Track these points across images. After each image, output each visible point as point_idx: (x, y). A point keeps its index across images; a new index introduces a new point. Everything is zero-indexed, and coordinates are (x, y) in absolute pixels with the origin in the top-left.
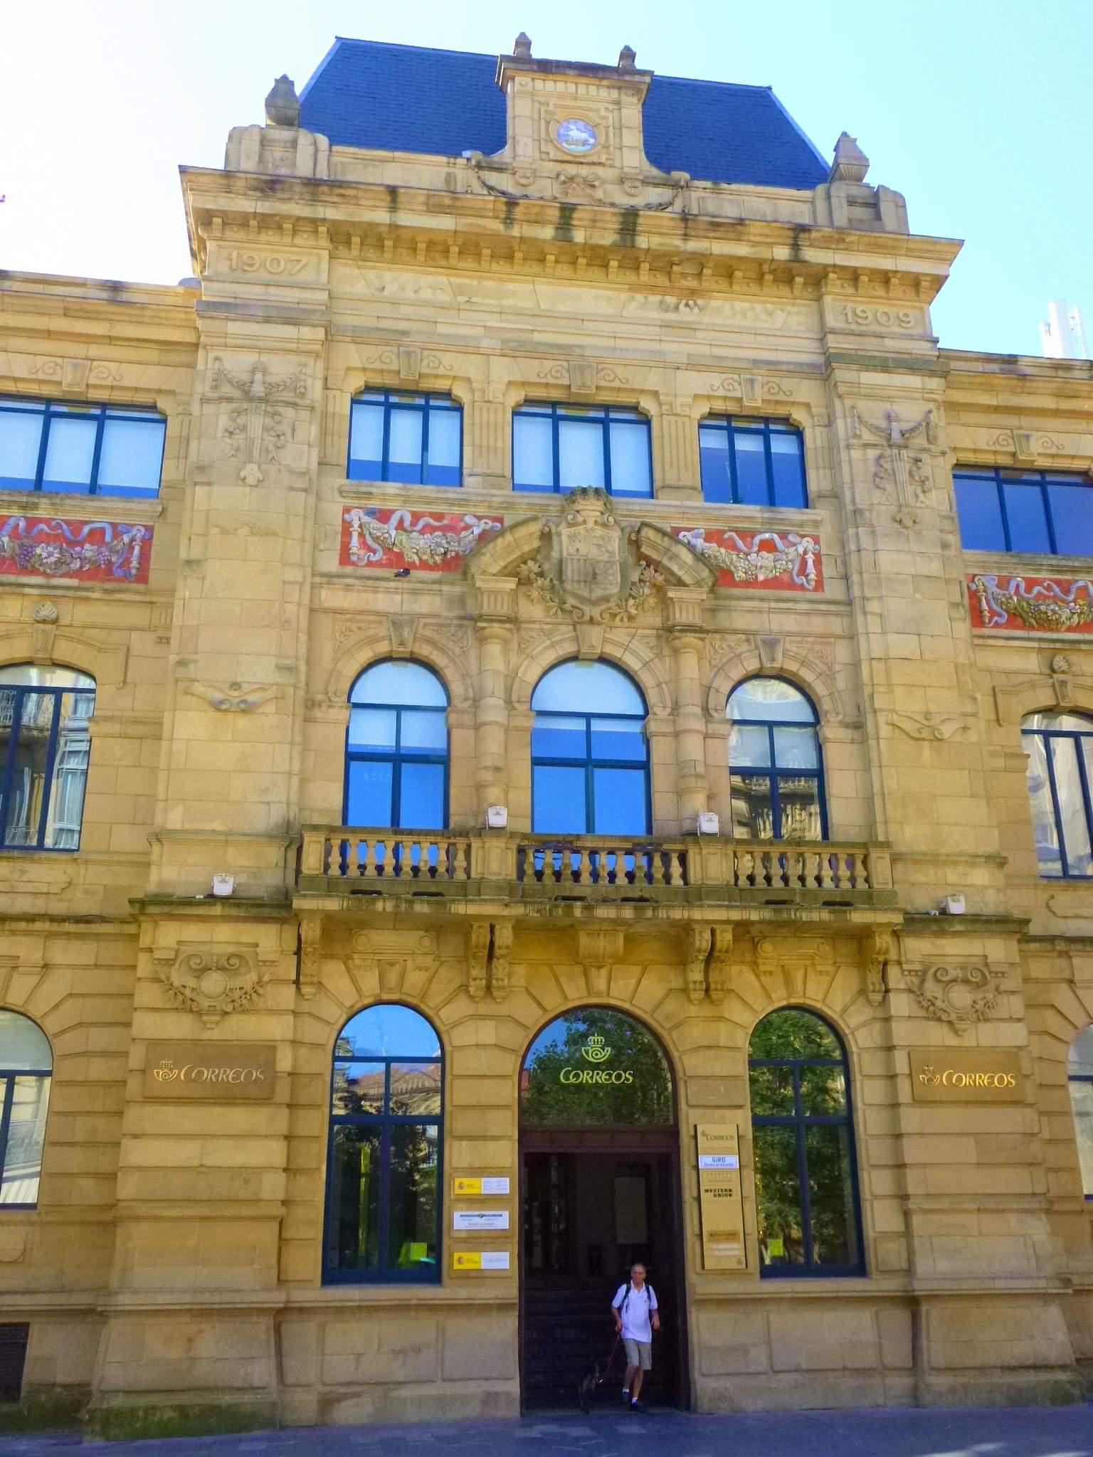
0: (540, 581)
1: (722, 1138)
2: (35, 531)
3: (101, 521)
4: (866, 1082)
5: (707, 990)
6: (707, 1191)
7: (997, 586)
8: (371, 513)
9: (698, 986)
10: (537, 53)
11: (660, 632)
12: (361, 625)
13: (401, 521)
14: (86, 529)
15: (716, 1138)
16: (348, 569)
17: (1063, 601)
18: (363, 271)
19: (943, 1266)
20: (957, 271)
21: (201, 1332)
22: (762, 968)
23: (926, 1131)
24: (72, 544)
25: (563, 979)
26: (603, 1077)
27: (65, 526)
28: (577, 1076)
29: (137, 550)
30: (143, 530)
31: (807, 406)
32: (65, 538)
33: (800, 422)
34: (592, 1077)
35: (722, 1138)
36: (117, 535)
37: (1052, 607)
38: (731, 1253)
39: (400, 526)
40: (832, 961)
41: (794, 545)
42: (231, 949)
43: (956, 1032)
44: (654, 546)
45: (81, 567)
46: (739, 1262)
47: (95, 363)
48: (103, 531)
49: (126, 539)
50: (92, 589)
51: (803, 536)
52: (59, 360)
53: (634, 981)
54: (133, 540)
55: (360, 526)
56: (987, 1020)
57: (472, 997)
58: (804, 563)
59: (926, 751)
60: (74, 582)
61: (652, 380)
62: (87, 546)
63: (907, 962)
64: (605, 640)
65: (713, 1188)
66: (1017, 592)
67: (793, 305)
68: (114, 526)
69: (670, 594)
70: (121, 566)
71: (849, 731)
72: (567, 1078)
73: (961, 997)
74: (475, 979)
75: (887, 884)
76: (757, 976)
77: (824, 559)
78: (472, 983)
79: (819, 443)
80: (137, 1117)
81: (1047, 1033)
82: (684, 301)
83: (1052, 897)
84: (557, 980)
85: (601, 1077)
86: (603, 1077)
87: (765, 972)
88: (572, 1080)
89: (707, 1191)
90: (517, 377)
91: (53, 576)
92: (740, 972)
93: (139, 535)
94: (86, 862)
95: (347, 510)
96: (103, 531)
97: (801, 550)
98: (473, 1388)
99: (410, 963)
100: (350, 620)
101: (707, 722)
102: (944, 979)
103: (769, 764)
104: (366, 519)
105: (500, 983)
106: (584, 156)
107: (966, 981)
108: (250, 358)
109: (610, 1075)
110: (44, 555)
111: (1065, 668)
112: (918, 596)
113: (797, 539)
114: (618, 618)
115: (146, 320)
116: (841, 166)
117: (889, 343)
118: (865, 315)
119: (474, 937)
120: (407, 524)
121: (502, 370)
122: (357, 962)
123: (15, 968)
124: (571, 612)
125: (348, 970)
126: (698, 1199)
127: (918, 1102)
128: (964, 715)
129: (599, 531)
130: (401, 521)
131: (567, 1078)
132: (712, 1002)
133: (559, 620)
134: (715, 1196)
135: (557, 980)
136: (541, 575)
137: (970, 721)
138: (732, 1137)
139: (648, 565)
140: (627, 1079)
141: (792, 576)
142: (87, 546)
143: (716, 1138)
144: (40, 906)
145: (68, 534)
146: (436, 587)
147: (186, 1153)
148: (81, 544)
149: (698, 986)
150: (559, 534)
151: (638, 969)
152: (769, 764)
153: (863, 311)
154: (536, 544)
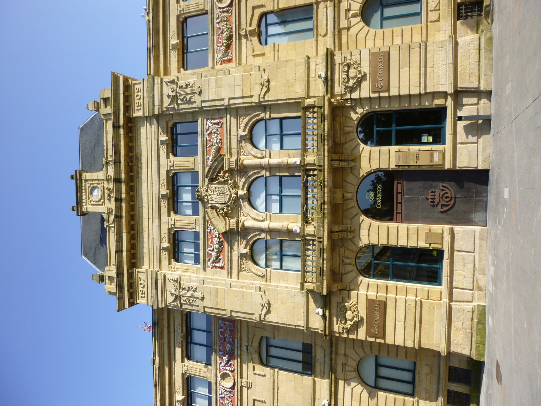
0: (225, 210)
1: (399, 157)
2: (222, 349)
3: (218, 332)
4: (381, 107)
5: (351, 161)
6: (417, 163)
7: (220, 54)
8: (209, 260)
9: (350, 164)
10: (75, 204)
11: (239, 172)
12: (242, 264)
13: (210, 250)
14: (221, 336)
15: (399, 159)
16: (226, 267)
17: (223, 30)
18: (141, 258)
19: (443, 80)
20: (122, 72)
21: (454, 326)
22: (344, 142)
23: (398, 87)
24: (225, 340)
25: (348, 207)
26: (379, 194)
27: (220, 342)
28: (379, 203)
29: (226, 323)
30: (220, 321)
31: (167, 123)
32: (223, 342)
33: (172, 124)
34: (379, 198)
35: (399, 157)
36: (222, 328)
37: (225, 35)
38: (437, 155)
39: (213, 251)
40: (342, 118)
41: (209, 126)
42: (339, 310)
43: (364, 77)
44: (212, 174)
45: (232, 338)
46: (440, 152)
47: (175, 330)
48: (221, 332)
49: (223, 325)
50: (238, 336)
51: (206, 124)
52: (175, 340)
53: (349, 185)
54: (223, 323)
55: (213, 263)
56: (360, 64)
57: (354, 237)
58: (215, 124)
59: (272, 84)
60: (236, 340)
61: (163, 172)
62: (225, 336)
63: (341, 92)
64: (243, 189)
65: (416, 161)
66: (221, 46)
67: (137, 126)
68: (219, 328)
69: (227, 169)
70: (231, 327)
71: (267, 110)
72: (379, 206)
73: (352, 72)
74: (348, 236)
75: (315, 101)
76: (346, 143)
77: (213, 117)
78: (349, 237)
79: (178, 118)
80: (389, 340)
81: (365, 38)
82: (140, 161)
83: (320, 35)
84: (348, 209)
85: (379, 195)
86: (379, 194)
87: (345, 141)
88: (380, 204)
89: (417, 163)
90: (166, 214)
91: (234, 345)
92: (345, 149)
93: (221, 322)
94: (315, 342)
95: (208, 267)
96: (221, 332)
97: (210, 125)
98: (477, 241)
99: (343, 256)
100: (241, 267)
101: (266, 158)
102: (347, 80)
103: (279, 136)
104: (211, 261)
105: (349, 228)
106: (102, 191)
107: (348, 71)
108: (169, 294)
109: (378, 192)
110: (229, 348)
111: (244, 30)
112: (222, 86)
113: (207, 126)
114: (235, 186)
115: (162, 317)
116: (96, 109)
117: (146, 95)
118: (138, 103)
119: (335, 238)
120: (211, 249)
121: (165, 217)
122: (343, 272)
123: (346, 364)
124: (234, 201)
125: (345, 274)
126: (419, 166)
127: (388, 90)
128: (259, 70)
129: (210, 192)
130: (210, 250)
131: (379, 206)
132: (355, 159)
133: (237, 204)
134: (418, 160)
135: (348, 209)
136: (223, 209)
137: (262, 69)
138: (399, 154)
139: (219, 176)
140: (380, 186)
141: (219, 128)
142: (225, 336)
143: (399, 159)
144: (327, 356)
145: (223, 341)
146: (229, 242)
147: (400, 325)
148: (225, 338)
149: (350, 164)
150: (211, 204)
151: (345, 183)
152: (279, 136)
153: (137, 103)
154: (214, 211)
